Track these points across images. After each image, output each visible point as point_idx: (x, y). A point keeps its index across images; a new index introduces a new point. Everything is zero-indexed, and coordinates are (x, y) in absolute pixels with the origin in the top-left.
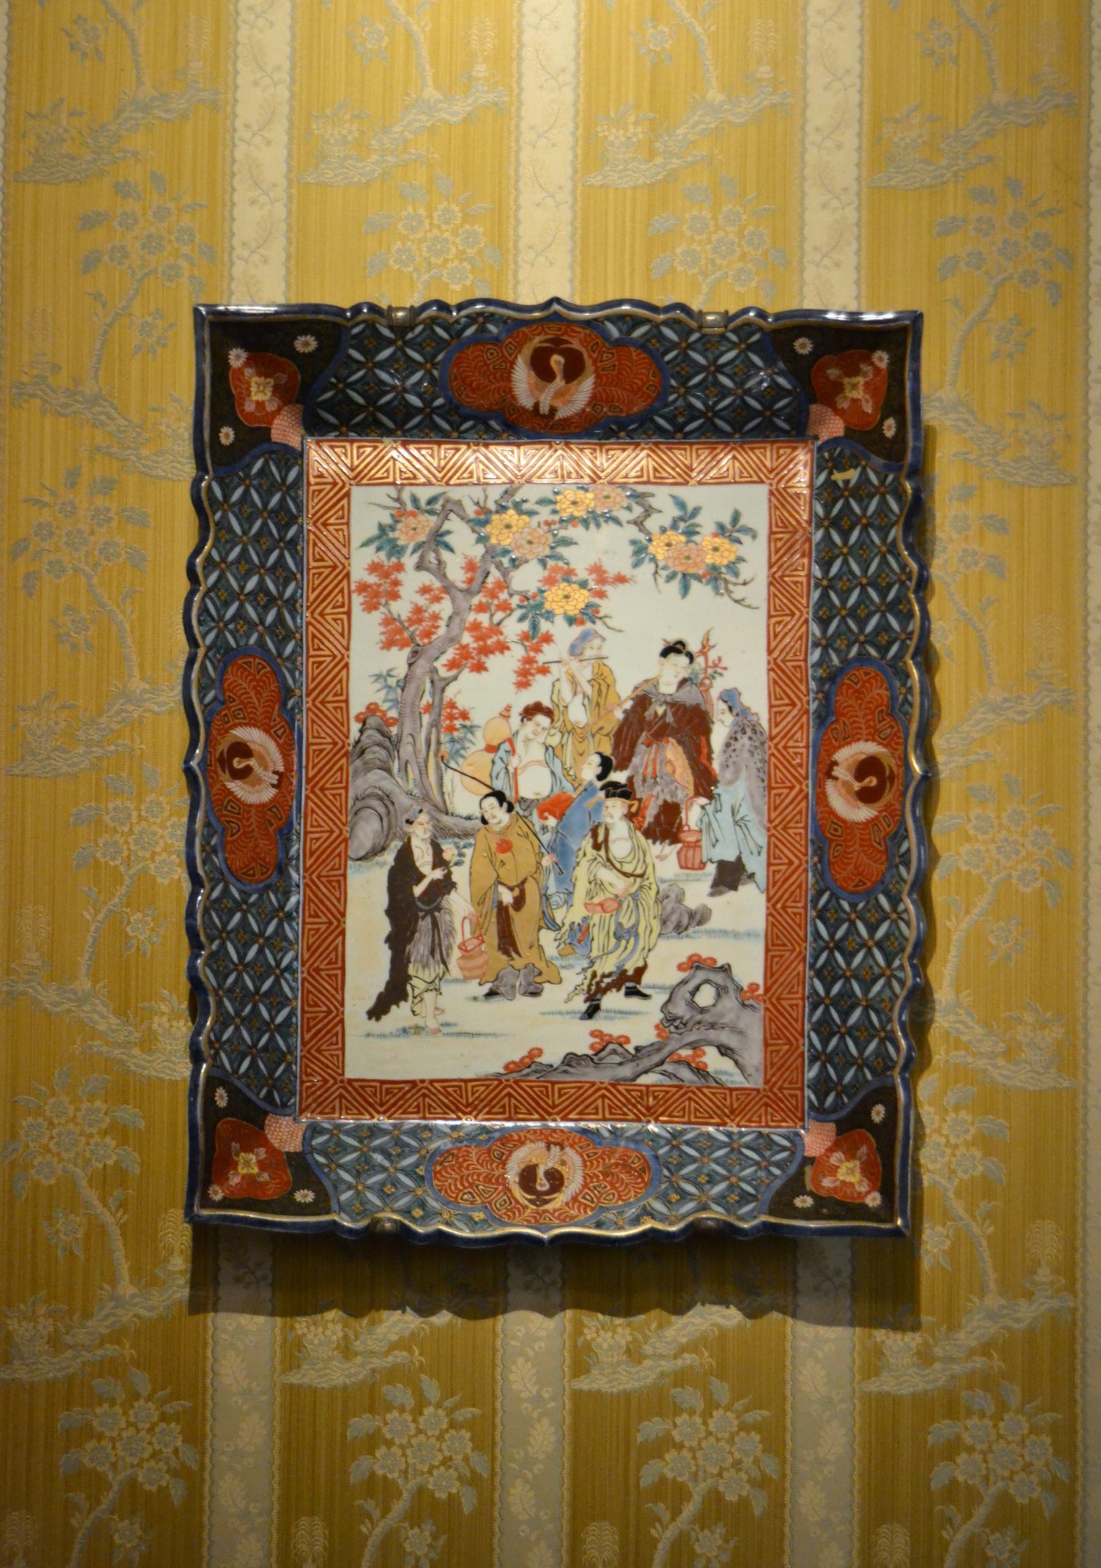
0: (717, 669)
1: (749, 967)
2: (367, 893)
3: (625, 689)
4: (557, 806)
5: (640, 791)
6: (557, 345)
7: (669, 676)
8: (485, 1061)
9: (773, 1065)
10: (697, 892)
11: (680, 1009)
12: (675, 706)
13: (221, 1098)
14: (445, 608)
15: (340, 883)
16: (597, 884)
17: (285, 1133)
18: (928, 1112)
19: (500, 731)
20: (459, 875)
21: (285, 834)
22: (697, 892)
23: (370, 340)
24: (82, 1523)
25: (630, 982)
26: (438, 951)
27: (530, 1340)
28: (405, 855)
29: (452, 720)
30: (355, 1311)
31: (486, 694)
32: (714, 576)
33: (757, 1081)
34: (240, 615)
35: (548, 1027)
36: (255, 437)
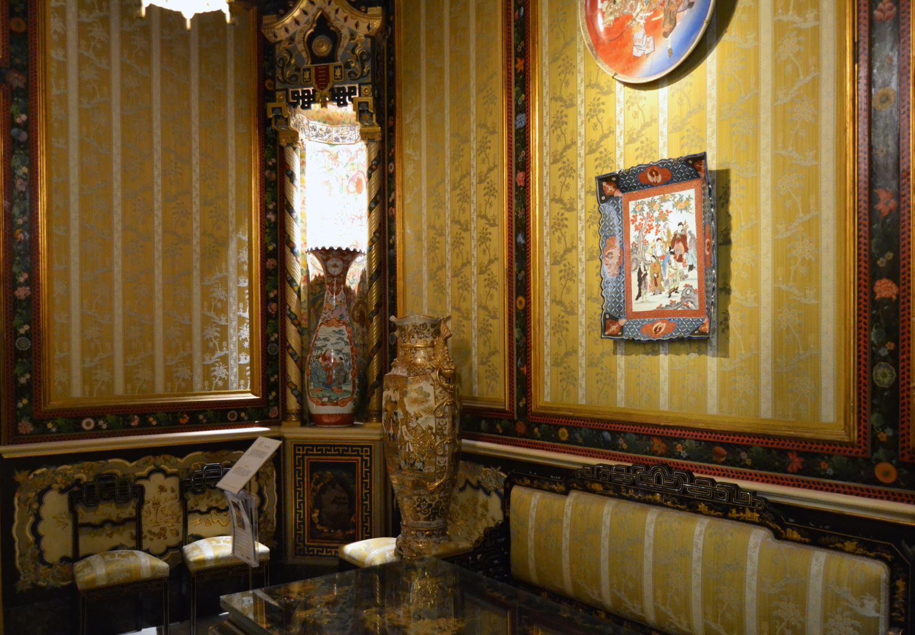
0: (687, 227)
1: (695, 286)
3: (672, 233)
4: (663, 257)
6: (653, 170)
8: (652, 307)
9: (701, 305)
13: (607, 316)
15: (630, 276)
17: (622, 322)
20: (648, 272)
22: (686, 271)
23: (624, 176)
25: (676, 290)
26: (645, 287)
27: (664, 360)
28: (640, 270)
31: (651, 237)
32: (686, 209)
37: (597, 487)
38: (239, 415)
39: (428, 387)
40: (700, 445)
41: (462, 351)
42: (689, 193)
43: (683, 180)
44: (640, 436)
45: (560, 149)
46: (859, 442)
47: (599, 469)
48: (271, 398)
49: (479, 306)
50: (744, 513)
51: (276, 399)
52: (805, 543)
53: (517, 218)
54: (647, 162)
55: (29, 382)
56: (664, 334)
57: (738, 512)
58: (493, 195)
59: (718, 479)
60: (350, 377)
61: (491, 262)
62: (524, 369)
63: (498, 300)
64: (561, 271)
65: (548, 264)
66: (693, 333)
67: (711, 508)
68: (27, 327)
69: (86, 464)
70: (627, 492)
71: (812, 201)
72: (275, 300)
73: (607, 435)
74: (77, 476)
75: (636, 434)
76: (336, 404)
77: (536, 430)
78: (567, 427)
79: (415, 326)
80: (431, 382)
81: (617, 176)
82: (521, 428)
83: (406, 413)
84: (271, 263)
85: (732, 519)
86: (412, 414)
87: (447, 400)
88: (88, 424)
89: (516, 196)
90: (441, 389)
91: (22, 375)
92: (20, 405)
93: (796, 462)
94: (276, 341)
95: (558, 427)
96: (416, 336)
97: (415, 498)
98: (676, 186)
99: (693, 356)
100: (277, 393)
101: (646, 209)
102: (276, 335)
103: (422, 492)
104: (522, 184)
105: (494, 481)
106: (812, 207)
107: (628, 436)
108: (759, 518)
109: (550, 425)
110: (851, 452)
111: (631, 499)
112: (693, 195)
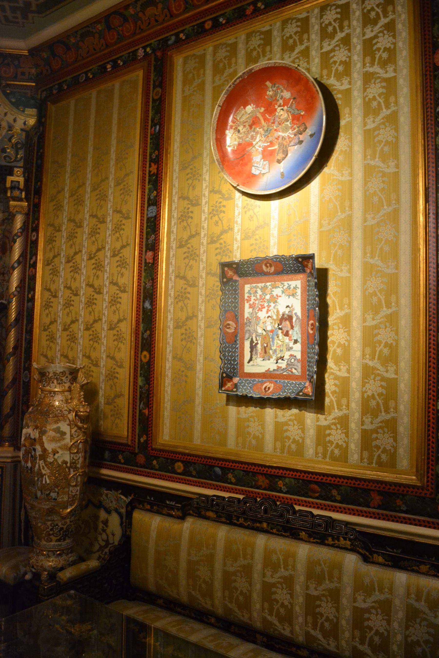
0: (294, 309)
1: (299, 356)
2: (247, 345)
3: (281, 313)
4: (272, 331)
5: (283, 329)
7: (287, 311)
9: (303, 371)
10: (291, 344)
11: (289, 362)
12: (288, 316)
13: (224, 375)
14: (257, 302)
16: (277, 343)
17: (236, 380)
18: (327, 380)
19: (264, 320)
20: (259, 342)
21: (236, 336)
22: (291, 344)
24: (287, 444)
25: (282, 358)
26: (256, 353)
28: (252, 339)
29: (258, 318)
30: (247, 407)
31: (262, 314)
32: (293, 295)
33: (300, 374)
34: (228, 305)
35: (269, 365)
36: (230, 280)
37: (211, 514)
39: (65, 427)
40: (298, 482)
41: (90, 393)
42: (297, 283)
43: (292, 273)
44: (247, 472)
45: (186, 237)
46: (428, 486)
47: (213, 500)
49: (108, 356)
50: (338, 540)
52: (388, 566)
53: (145, 288)
54: (262, 255)
56: (272, 393)
57: (333, 540)
58: (125, 267)
59: (316, 512)
61: (120, 321)
62: (146, 412)
63: (125, 352)
64: (182, 334)
65: (171, 327)
66: (298, 394)
67: (310, 536)
70: (238, 521)
71: (393, 299)
73: (218, 470)
75: (243, 471)
77: (155, 462)
78: (182, 462)
79: (55, 374)
81: (237, 264)
82: (141, 459)
83: (44, 450)
85: (328, 545)
86: (50, 451)
89: (145, 270)
90: (76, 428)
93: (377, 499)
95: (174, 461)
96: (55, 381)
97: (49, 523)
98: (285, 277)
99: (295, 411)
101: (259, 292)
103: (55, 518)
104: (151, 261)
105: (114, 503)
106: (393, 304)
107: (236, 472)
108: (351, 545)
109: (167, 459)
110: (421, 493)
111: (241, 526)
112: (299, 286)
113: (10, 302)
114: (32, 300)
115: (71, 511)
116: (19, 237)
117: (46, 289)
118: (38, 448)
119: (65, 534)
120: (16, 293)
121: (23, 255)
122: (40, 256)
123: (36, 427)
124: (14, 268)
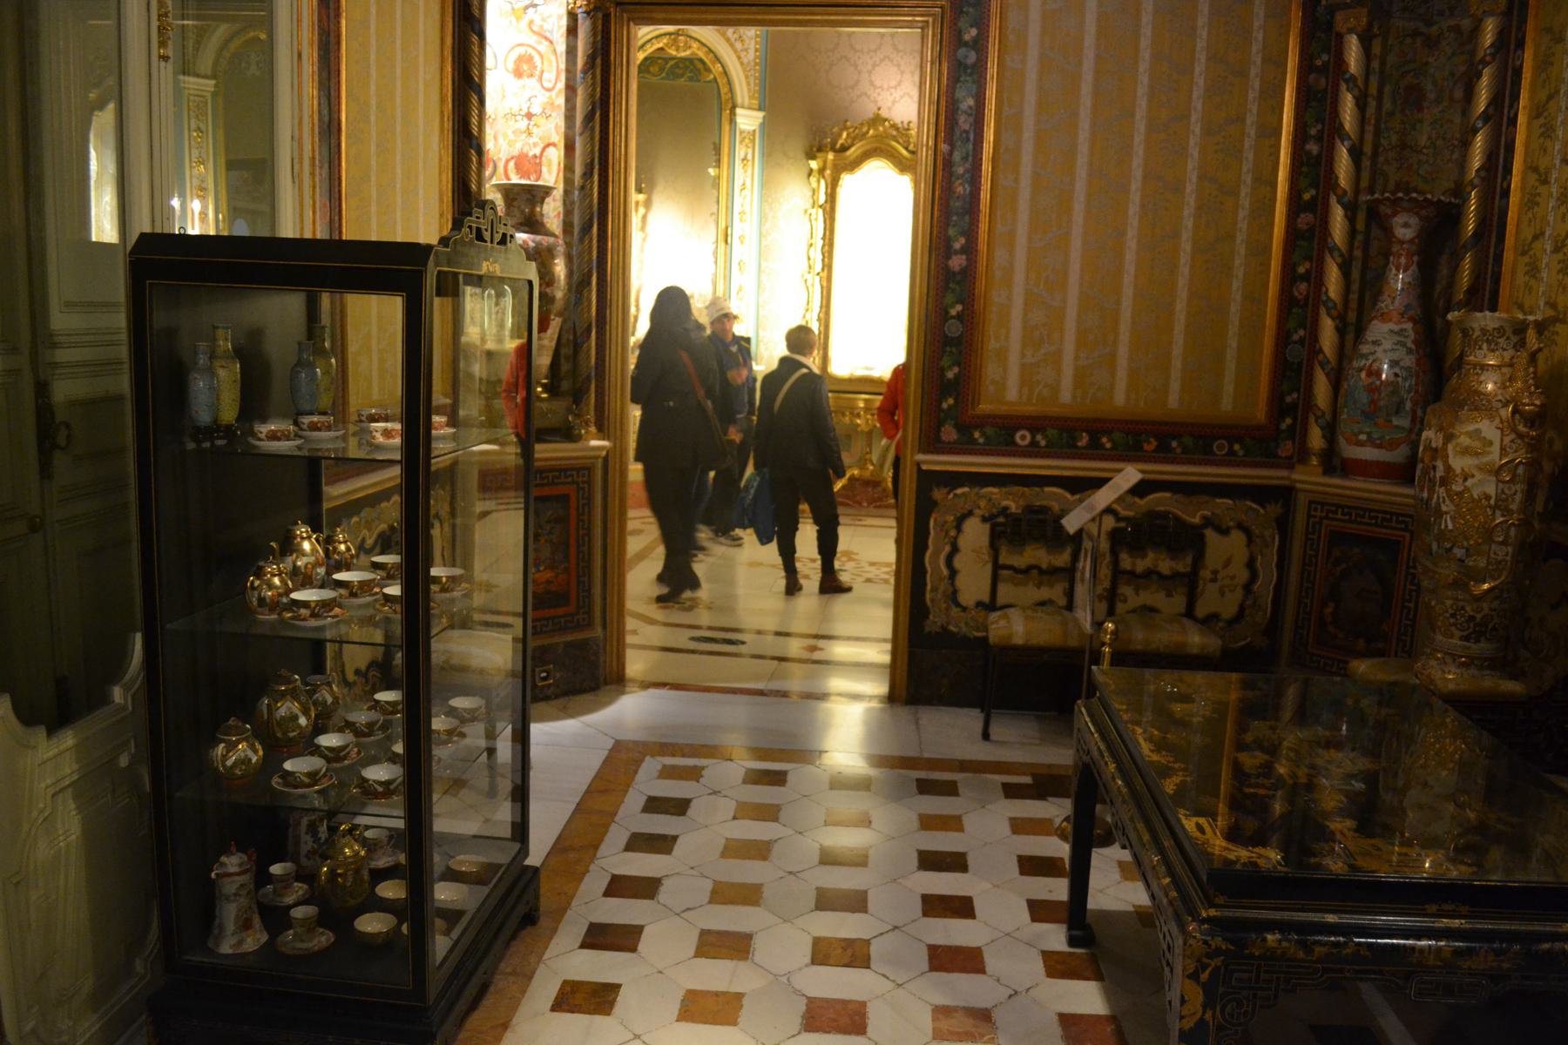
38: (1231, 447)
39: (1488, 429)
48: (1284, 426)
51: (1292, 428)
55: (957, 377)
60: (1408, 405)
68: (959, 308)
69: (1016, 489)
72: (1306, 277)
74: (1005, 503)
76: (1380, 446)
79: (1484, 331)
80: (1497, 421)
83: (1449, 468)
84: (1305, 220)
87: (1521, 456)
88: (1023, 437)
90: (1513, 436)
91: (950, 368)
92: (945, 406)
94: (1301, 341)
96: (1485, 346)
97: (1448, 602)
100: (1295, 419)
102: (1301, 332)
113: (1466, 200)
114: (1506, 193)
115: (1489, 590)
116: (1488, 64)
117: (1531, 168)
118: (1439, 464)
119: (1476, 631)
120: (1476, 181)
121: (1496, 101)
122: (1523, 101)
123: (1441, 429)
124: (1475, 131)
